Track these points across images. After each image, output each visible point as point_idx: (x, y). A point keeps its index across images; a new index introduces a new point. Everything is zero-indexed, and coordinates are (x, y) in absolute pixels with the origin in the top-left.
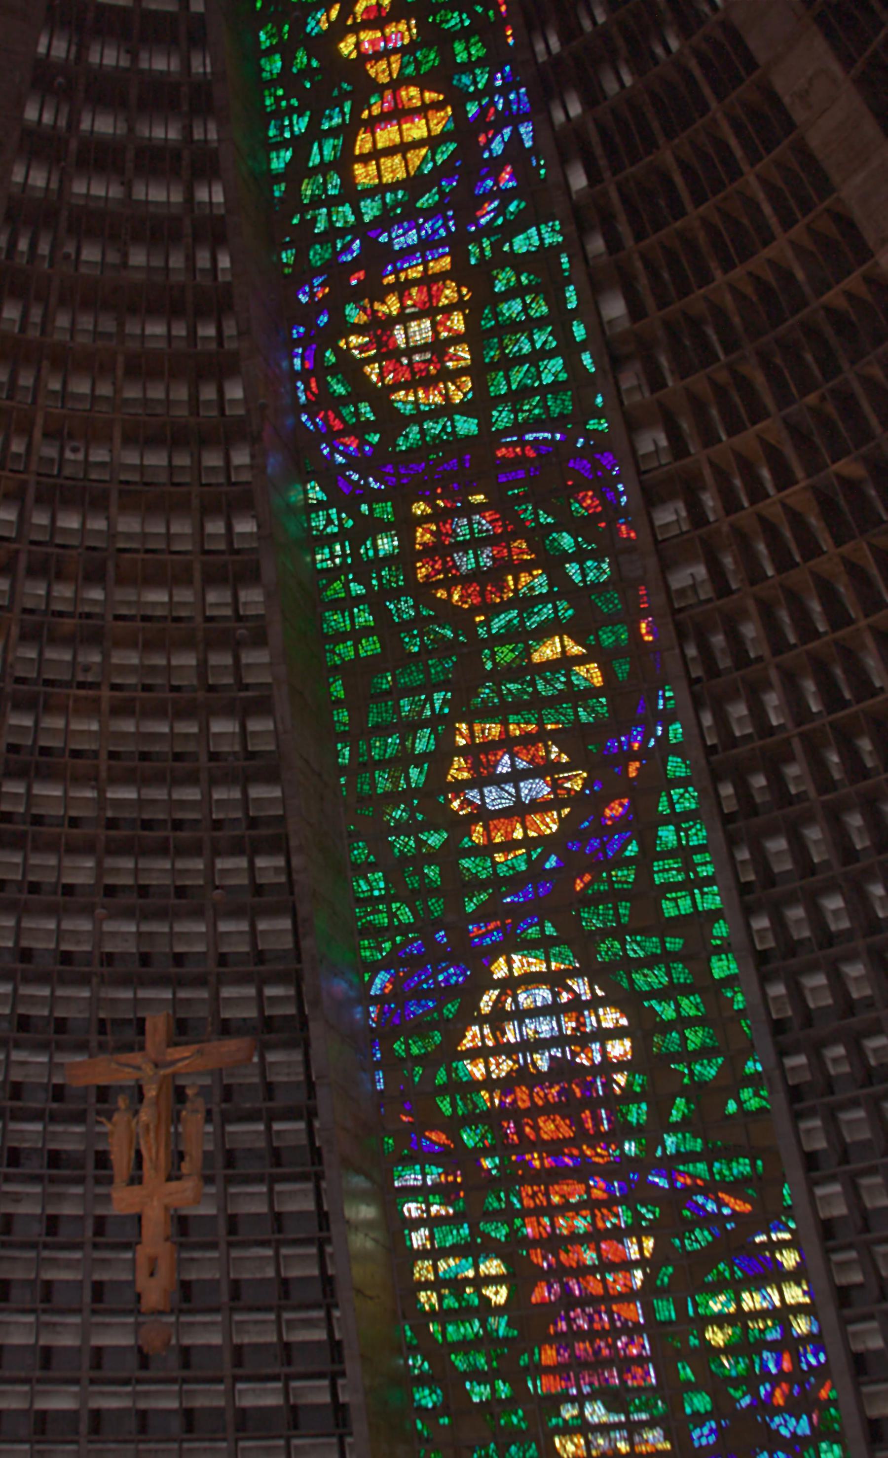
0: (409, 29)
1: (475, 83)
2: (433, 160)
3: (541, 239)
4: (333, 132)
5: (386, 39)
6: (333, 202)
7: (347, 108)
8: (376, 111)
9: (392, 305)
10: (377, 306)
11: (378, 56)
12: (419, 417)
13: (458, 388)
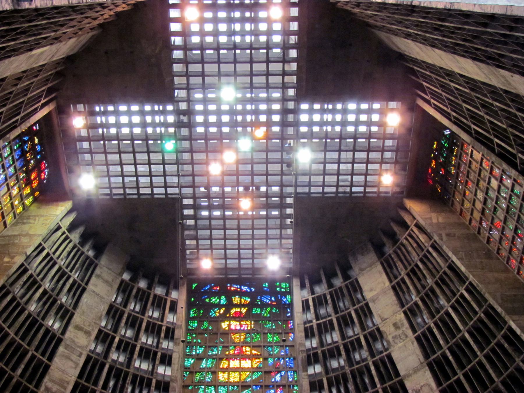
0: (251, 324)
1: (273, 351)
2: (251, 377)
4: (212, 357)
5: (241, 326)
7: (220, 348)
8: (232, 352)
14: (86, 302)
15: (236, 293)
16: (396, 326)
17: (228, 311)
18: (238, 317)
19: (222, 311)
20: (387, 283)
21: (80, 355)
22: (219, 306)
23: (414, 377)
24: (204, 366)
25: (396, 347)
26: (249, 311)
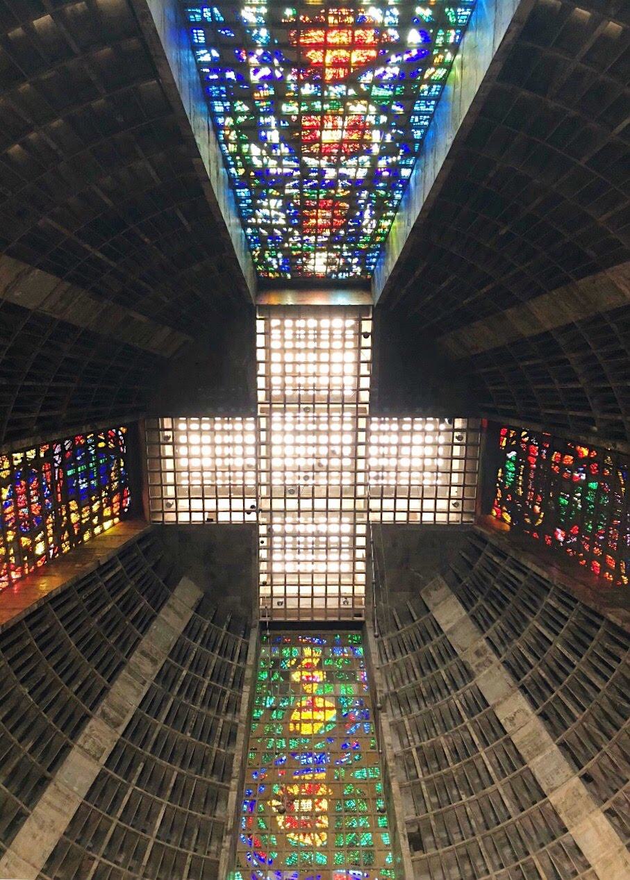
2: (325, 729)
3: (368, 774)
6: (279, 737)
8: (304, 704)
9: (295, 790)
10: (288, 788)
11: (308, 682)
12: (298, 848)
13: (320, 838)
14: (155, 629)
15: (307, 644)
16: (478, 654)
17: (299, 661)
18: (309, 667)
19: (293, 663)
20: (464, 613)
21: (144, 683)
22: (291, 659)
23: (506, 704)
24: (275, 717)
25: (481, 676)
26: (320, 664)
